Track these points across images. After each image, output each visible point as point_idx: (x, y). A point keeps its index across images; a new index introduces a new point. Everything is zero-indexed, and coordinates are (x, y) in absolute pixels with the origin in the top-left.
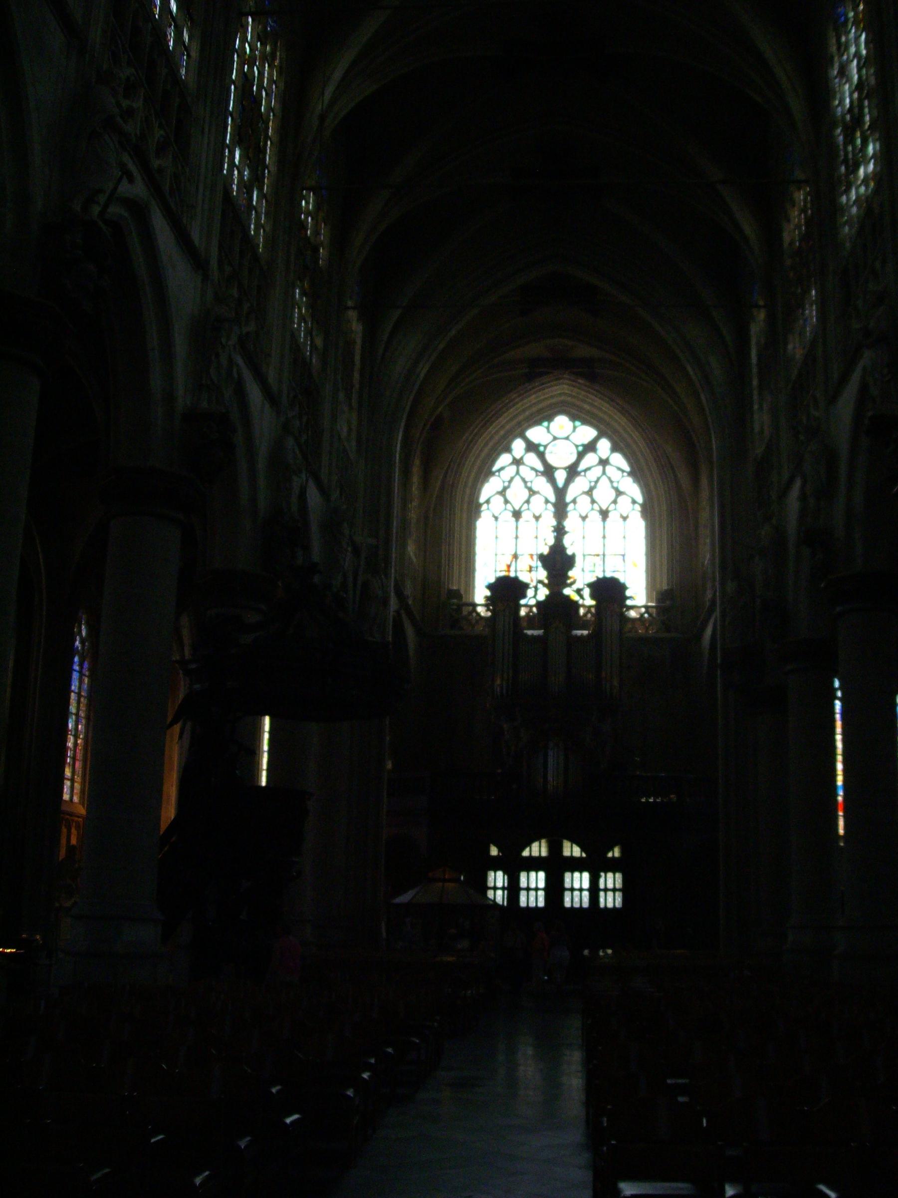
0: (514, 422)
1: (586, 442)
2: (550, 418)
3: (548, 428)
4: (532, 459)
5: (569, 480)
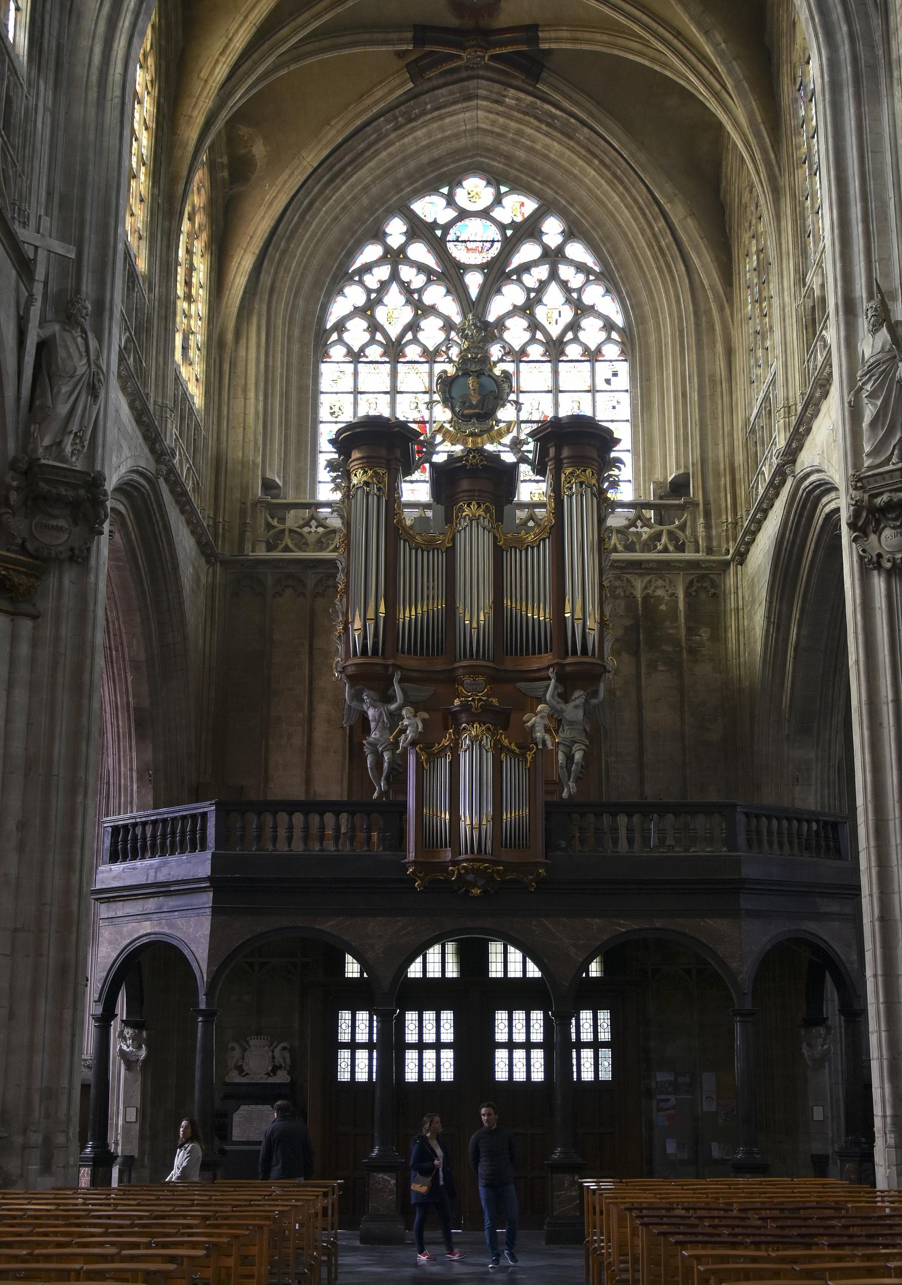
1: (519, 219)
4: (419, 252)
5: (491, 288)
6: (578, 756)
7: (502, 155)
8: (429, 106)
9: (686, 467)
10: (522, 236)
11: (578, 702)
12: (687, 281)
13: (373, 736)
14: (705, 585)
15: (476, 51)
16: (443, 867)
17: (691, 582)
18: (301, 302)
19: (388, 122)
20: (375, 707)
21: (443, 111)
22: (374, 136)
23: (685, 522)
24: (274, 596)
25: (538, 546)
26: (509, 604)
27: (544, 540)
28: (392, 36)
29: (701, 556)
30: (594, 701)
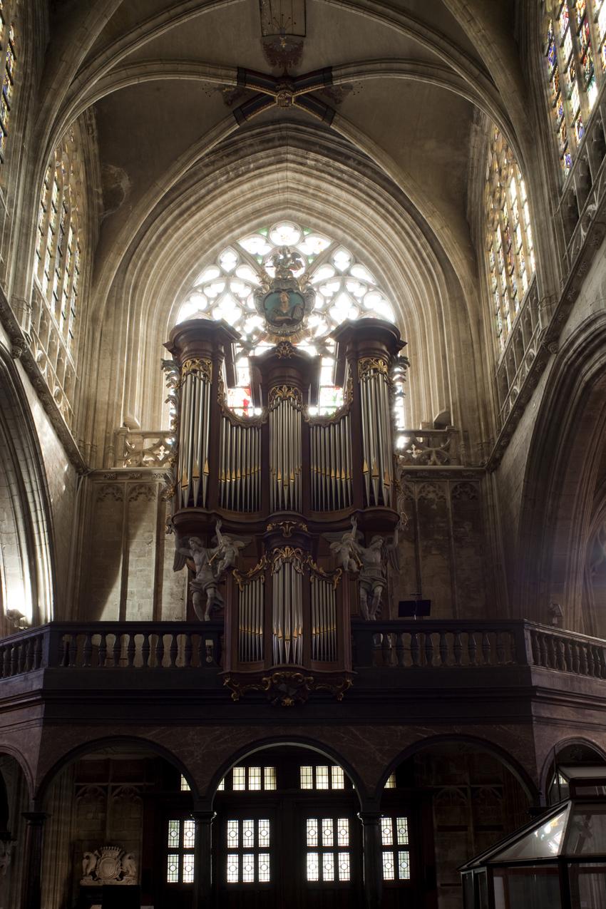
0: (223, 223)
1: (317, 252)
2: (269, 226)
3: (268, 236)
6: (379, 590)
7: (305, 207)
8: (252, 166)
9: (448, 407)
10: (320, 262)
11: (376, 545)
12: (443, 277)
13: (198, 577)
14: (466, 490)
15: (285, 94)
16: (256, 678)
17: (456, 487)
18: (158, 302)
19: (222, 175)
20: (200, 552)
21: (262, 170)
22: (212, 185)
23: (449, 445)
24: (130, 501)
25: (339, 424)
26: (315, 469)
29: (461, 467)
30: (391, 546)
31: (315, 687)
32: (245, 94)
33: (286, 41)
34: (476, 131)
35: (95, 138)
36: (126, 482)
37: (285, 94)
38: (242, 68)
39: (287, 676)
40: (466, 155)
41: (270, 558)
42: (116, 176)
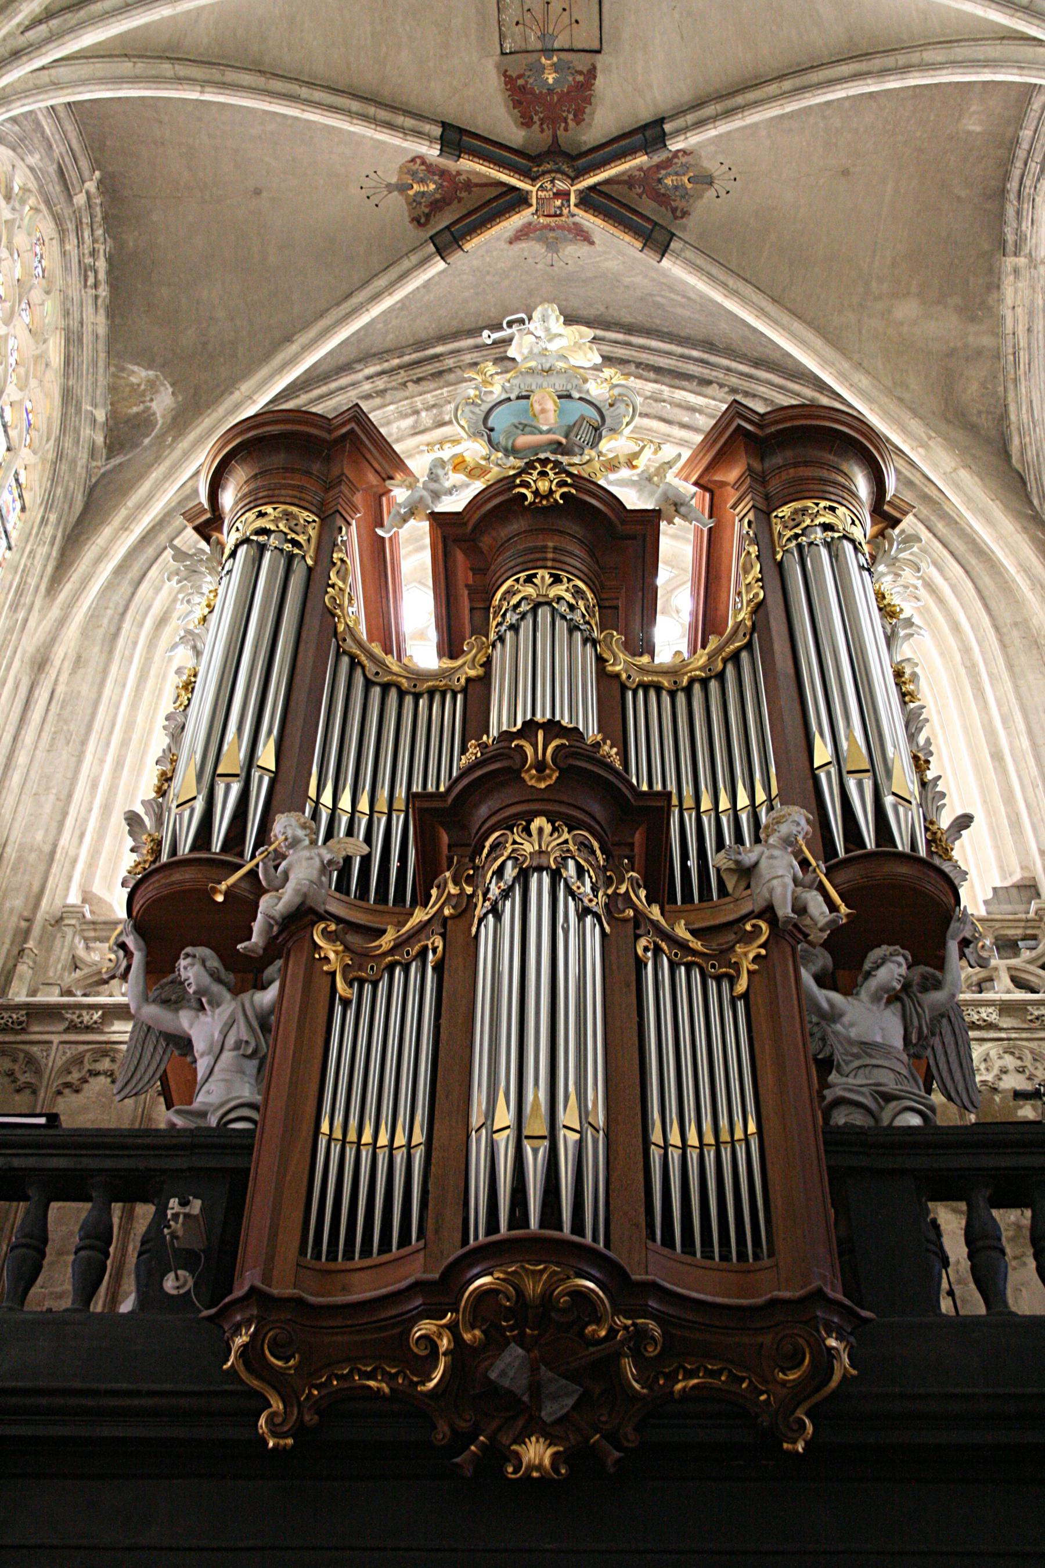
15: (552, 181)
19: (404, 416)
24: (59, 1093)
25: (721, 676)
27: (735, 657)
28: (400, 120)
31: (672, 1378)
32: (460, 200)
33: (556, 67)
34: (1016, 271)
35: (100, 301)
36: (56, 1039)
37: (552, 181)
38: (449, 124)
39: (533, 1288)
40: (996, 329)
41: (470, 880)
42: (143, 387)
